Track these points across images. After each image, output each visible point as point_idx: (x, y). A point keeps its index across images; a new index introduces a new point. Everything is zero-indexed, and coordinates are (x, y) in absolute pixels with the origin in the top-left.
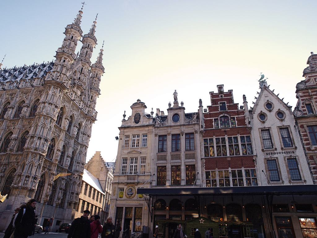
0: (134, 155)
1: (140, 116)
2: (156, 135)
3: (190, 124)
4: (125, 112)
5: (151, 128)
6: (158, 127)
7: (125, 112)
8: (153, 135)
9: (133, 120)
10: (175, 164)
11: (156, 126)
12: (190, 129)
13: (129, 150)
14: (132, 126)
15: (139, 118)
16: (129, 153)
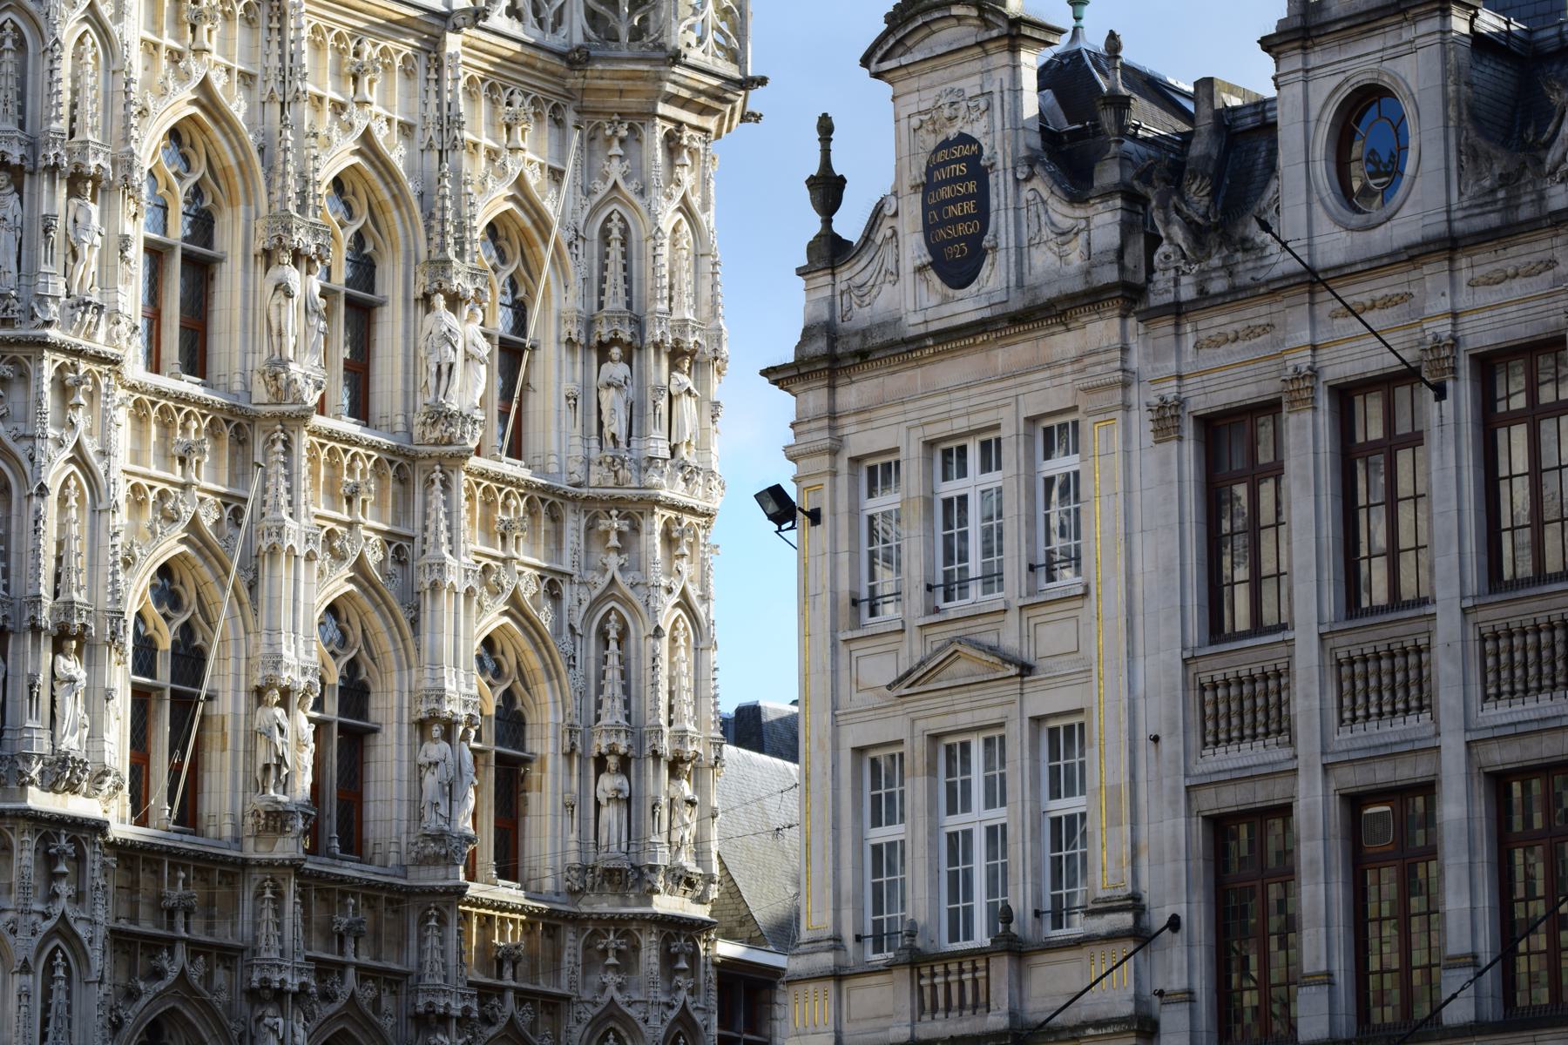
0: (961, 699)
1: (978, 172)
2: (1166, 420)
3: (1525, 213)
4: (826, 127)
5: (1102, 330)
6: (1178, 311)
7: (826, 127)
8: (1142, 423)
9: (913, 249)
10: (1383, 775)
11: (1160, 294)
12: (1518, 288)
13: (912, 650)
14: (913, 323)
15: (969, 207)
16: (911, 681)
